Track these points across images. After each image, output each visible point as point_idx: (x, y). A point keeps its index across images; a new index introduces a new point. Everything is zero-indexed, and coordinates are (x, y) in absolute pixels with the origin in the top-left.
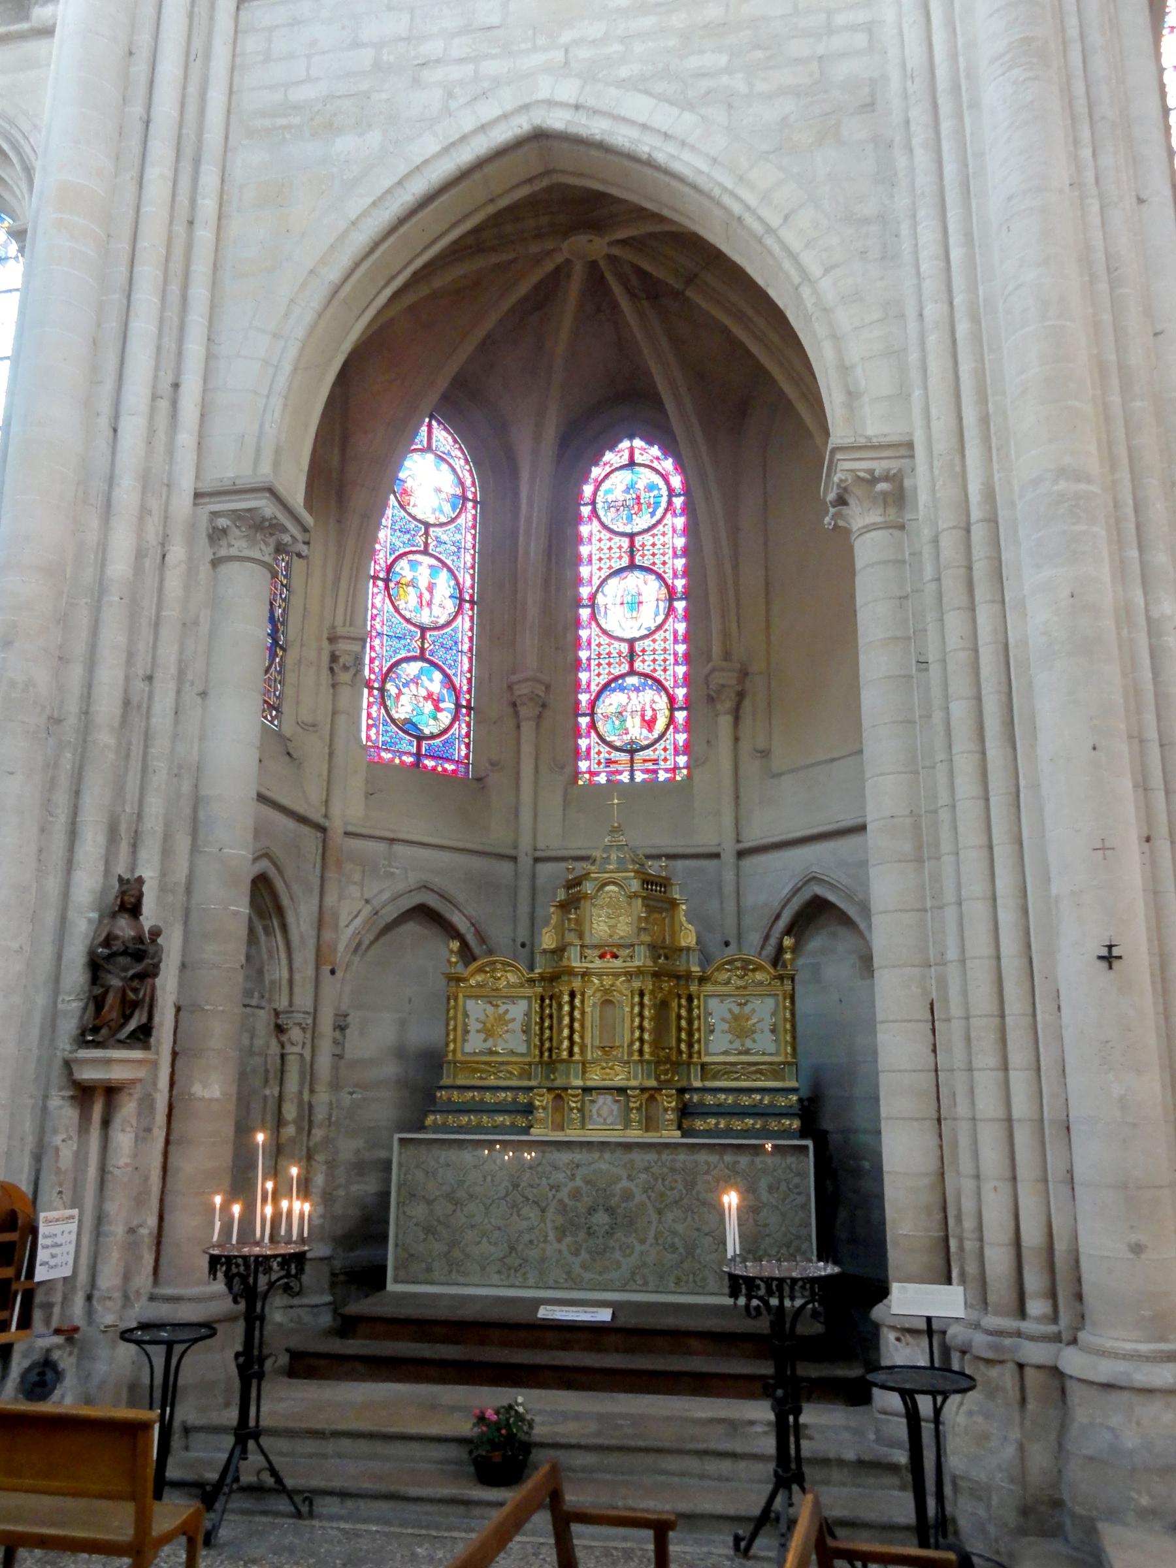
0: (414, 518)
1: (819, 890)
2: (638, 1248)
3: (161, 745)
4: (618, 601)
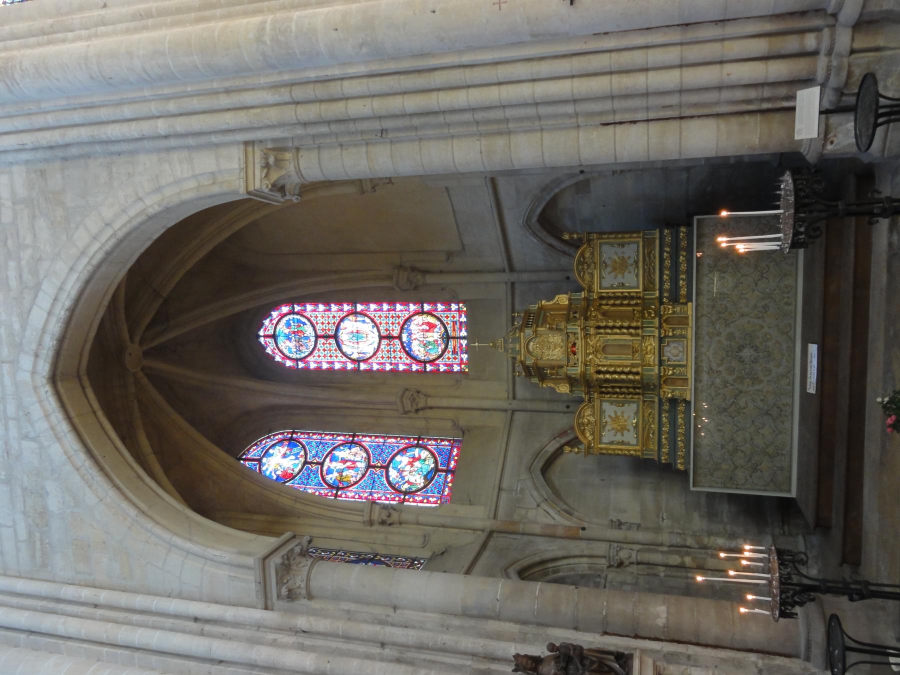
0: (300, 470)
3: (426, 637)
4: (356, 346)
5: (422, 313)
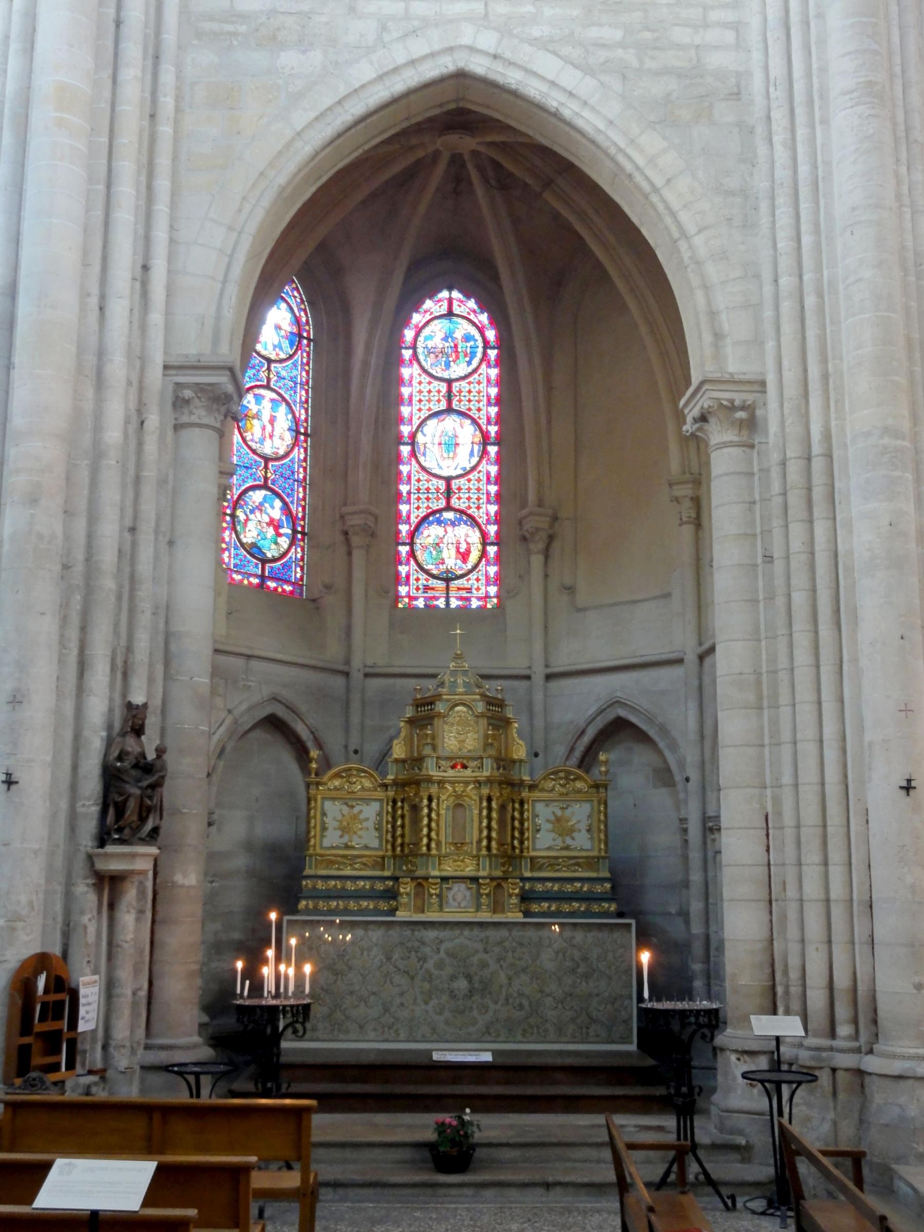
1: (622, 713)
2: (492, 1006)
4: (436, 441)
5: (485, 541)
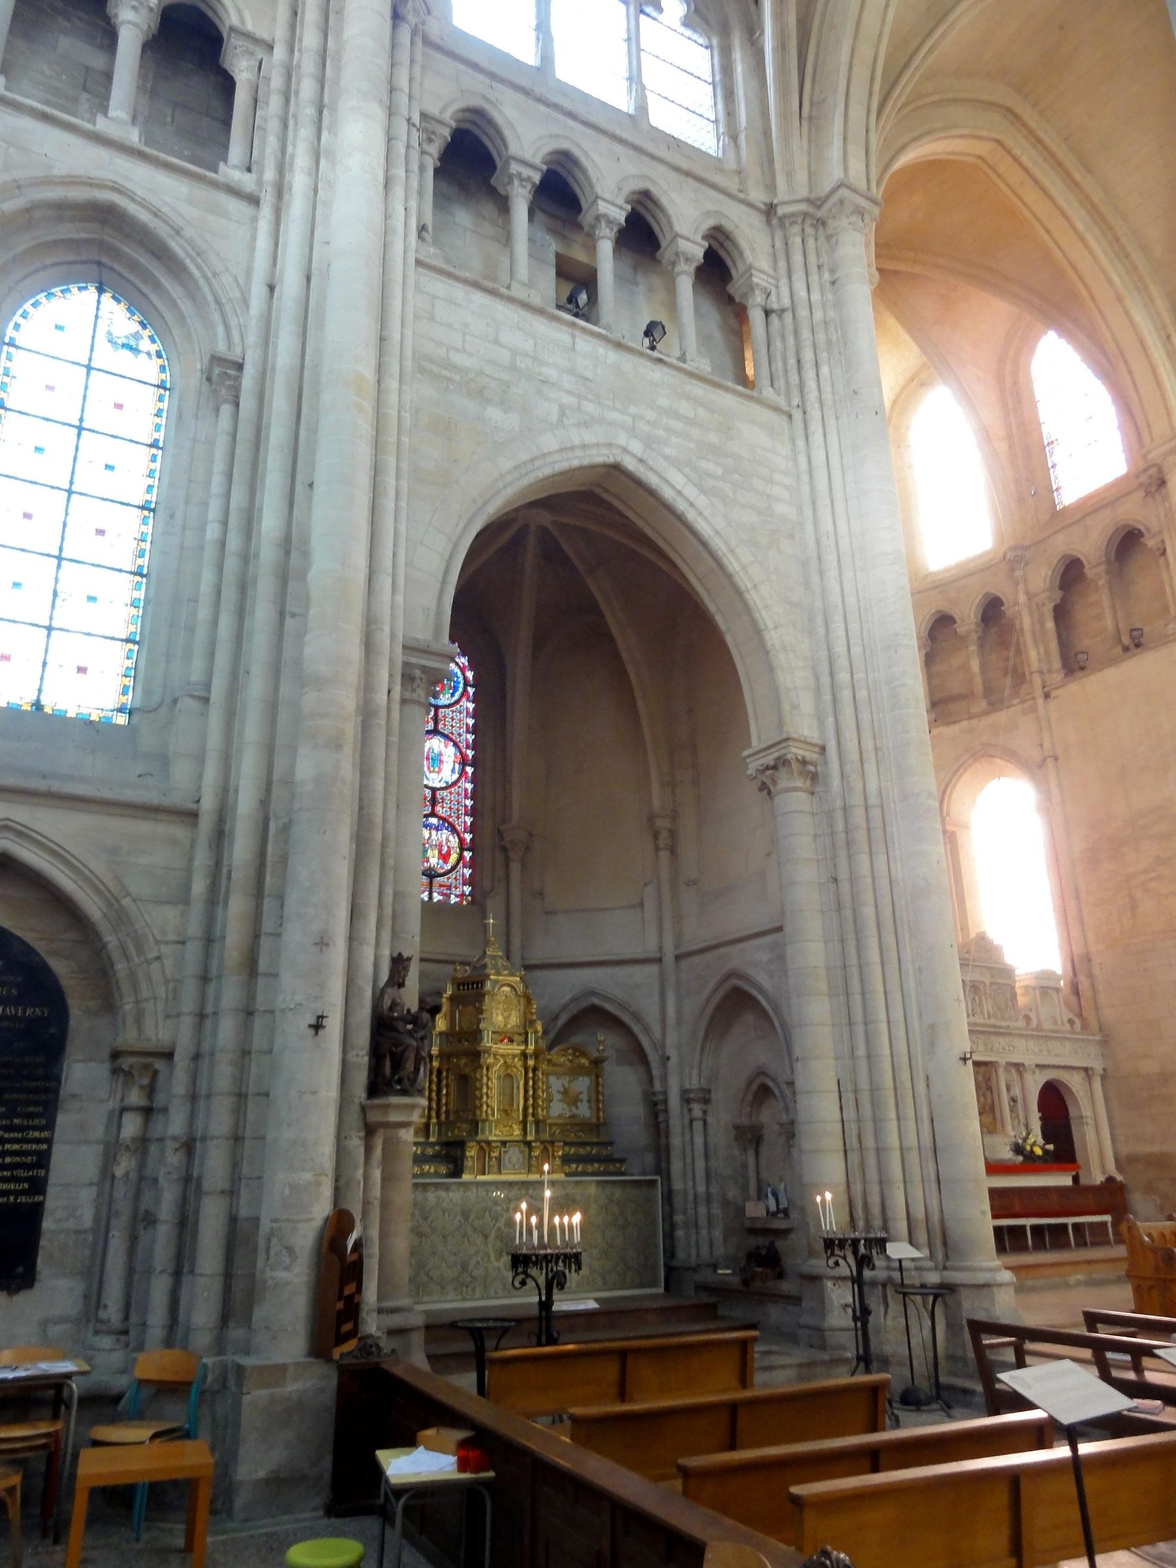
1: (596, 1001)
